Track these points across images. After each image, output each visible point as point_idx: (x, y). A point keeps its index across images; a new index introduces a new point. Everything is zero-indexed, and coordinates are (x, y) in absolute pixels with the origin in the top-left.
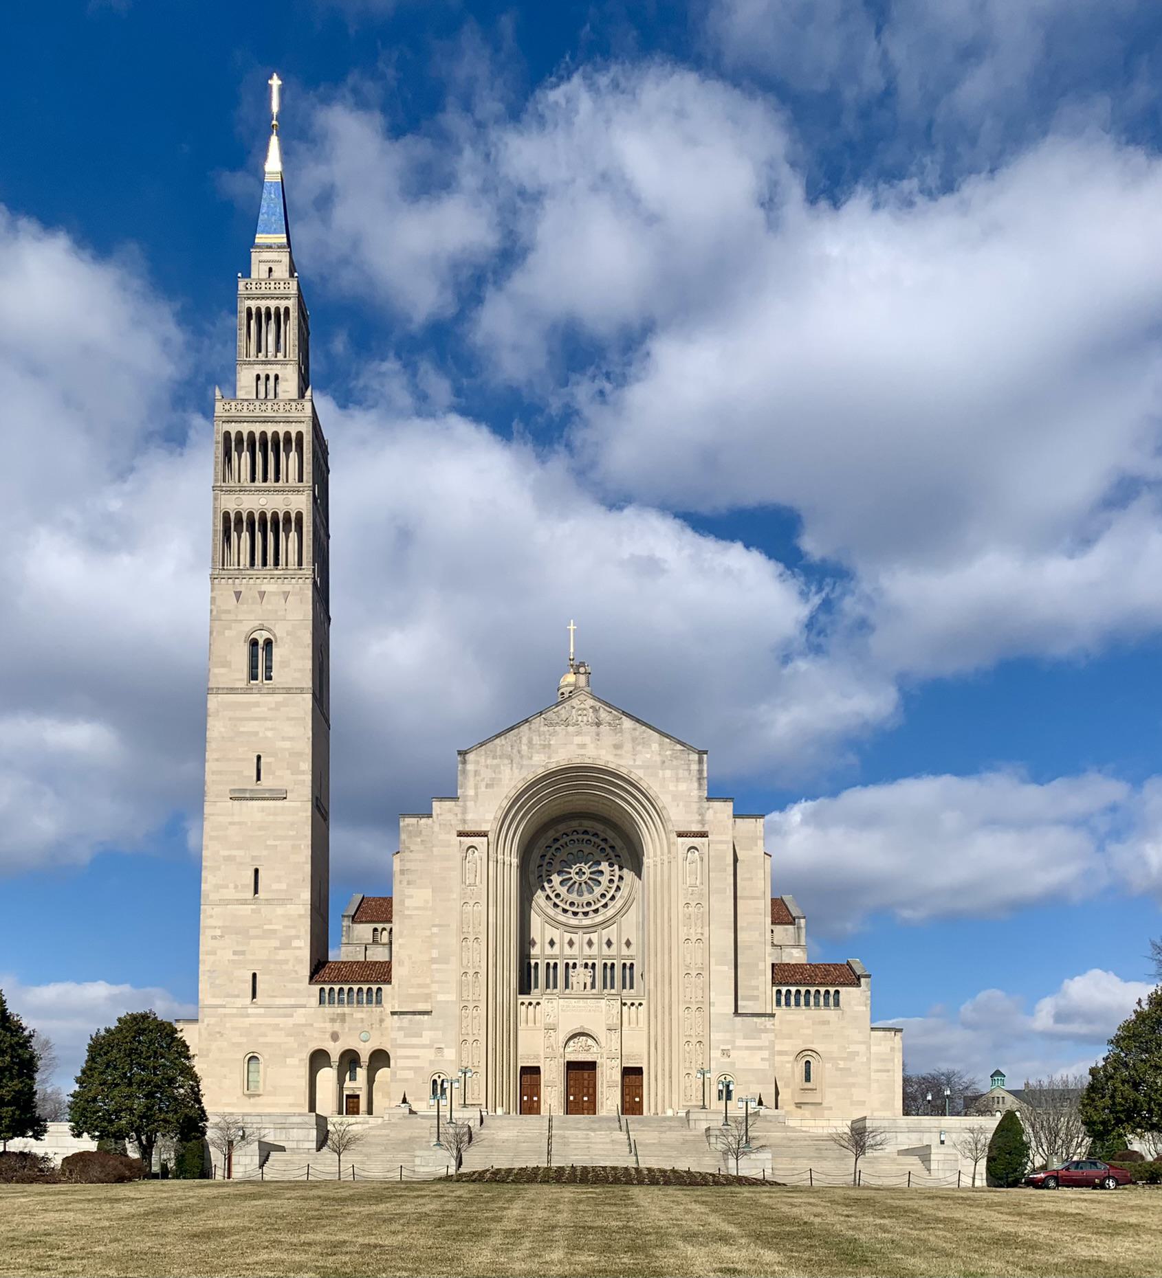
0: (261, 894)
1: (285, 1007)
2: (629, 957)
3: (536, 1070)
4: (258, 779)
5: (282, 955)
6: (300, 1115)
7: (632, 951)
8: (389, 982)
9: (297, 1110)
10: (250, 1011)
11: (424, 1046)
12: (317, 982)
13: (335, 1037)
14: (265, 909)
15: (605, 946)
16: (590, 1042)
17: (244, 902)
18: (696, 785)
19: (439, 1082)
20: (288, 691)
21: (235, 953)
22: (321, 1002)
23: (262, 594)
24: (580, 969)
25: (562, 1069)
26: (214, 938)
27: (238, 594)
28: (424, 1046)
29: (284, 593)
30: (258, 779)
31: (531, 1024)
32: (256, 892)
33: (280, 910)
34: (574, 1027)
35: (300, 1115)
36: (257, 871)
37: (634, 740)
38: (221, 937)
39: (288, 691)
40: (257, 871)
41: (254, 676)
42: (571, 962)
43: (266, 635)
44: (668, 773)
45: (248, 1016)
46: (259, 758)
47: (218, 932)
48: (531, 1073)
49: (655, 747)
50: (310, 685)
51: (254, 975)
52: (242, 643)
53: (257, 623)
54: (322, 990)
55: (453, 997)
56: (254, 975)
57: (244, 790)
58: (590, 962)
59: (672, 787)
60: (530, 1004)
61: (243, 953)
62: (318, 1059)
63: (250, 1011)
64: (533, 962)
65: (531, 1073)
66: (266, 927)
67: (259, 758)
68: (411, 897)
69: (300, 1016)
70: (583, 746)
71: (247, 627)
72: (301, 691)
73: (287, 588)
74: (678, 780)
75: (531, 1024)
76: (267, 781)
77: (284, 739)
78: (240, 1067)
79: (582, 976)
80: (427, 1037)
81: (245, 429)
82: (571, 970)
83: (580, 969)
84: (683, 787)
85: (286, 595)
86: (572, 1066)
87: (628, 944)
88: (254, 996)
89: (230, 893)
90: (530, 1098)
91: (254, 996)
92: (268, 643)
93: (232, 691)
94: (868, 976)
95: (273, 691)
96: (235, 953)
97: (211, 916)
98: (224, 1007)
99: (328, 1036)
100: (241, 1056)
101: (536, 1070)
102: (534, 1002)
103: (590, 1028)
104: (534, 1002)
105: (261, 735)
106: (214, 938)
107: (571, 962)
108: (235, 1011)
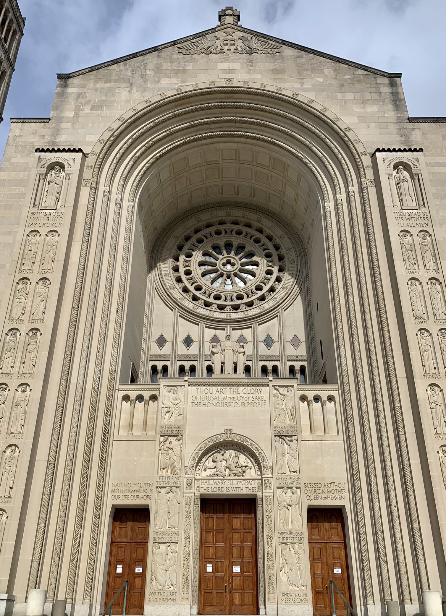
3: (141, 514)
16: (243, 459)
18: (391, 107)
25: (195, 511)
31: (137, 432)
34: (215, 430)
48: (132, 518)
60: (140, 398)
65: (132, 518)
75: (137, 432)
86: (209, 504)
90: (129, 568)
101: (141, 514)
102: (147, 395)
103: (242, 430)
104: (147, 395)
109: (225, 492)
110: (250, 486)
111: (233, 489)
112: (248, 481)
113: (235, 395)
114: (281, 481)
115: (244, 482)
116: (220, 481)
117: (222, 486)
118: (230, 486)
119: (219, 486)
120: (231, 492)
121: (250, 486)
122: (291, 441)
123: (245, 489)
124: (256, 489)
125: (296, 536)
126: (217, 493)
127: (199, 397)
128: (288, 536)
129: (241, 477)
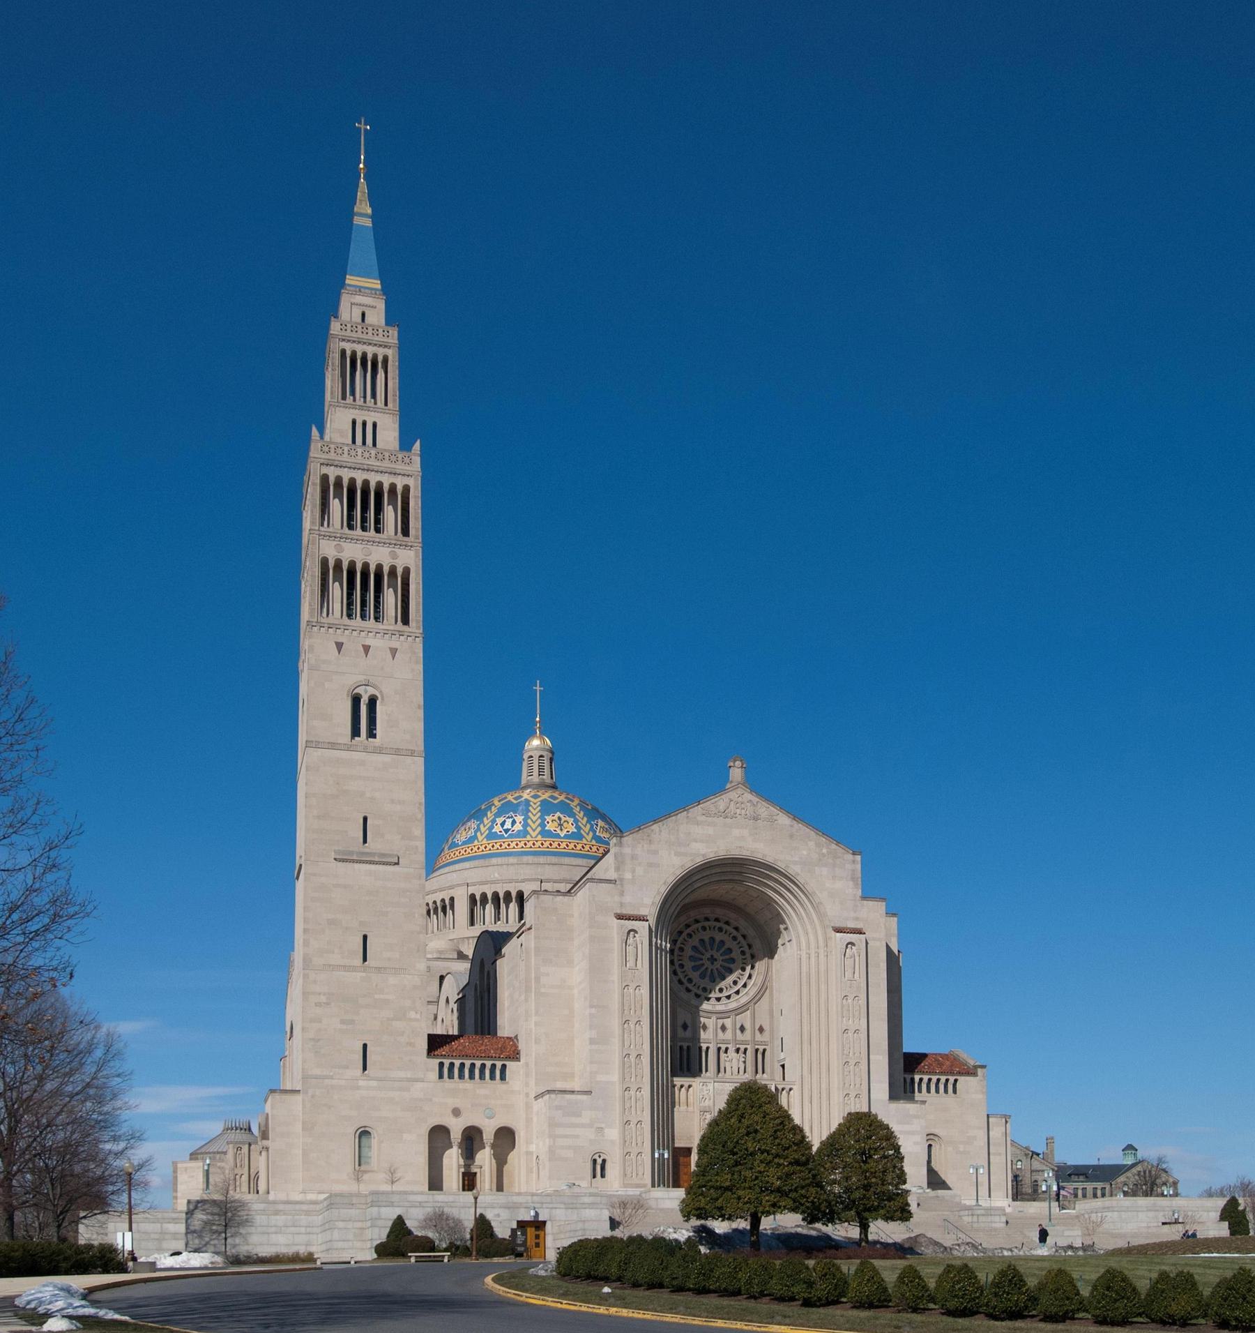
1: (401, 1080)
2: (762, 1043)
4: (365, 841)
5: (398, 1024)
6: (422, 1193)
7: (766, 1037)
8: (518, 1059)
9: (416, 1188)
10: (361, 1083)
11: (583, 1126)
12: (436, 1056)
13: (456, 1112)
15: (738, 1032)
17: (346, 968)
19: (599, 1161)
20: (397, 752)
21: (343, 1022)
22: (441, 1076)
23: (367, 649)
24: (732, 1053)
26: (318, 1004)
27: (339, 646)
28: (583, 1126)
29: (391, 649)
30: (365, 841)
32: (365, 959)
33: (392, 980)
35: (422, 1193)
36: (365, 937)
38: (328, 1004)
39: (397, 752)
40: (365, 937)
41: (356, 732)
42: (723, 1047)
43: (371, 691)
45: (358, 1088)
46: (365, 819)
47: (323, 999)
50: (422, 748)
51: (365, 1046)
52: (345, 696)
53: (361, 678)
54: (441, 1065)
55: (615, 1077)
56: (365, 1046)
57: (351, 853)
58: (742, 1047)
61: (352, 1022)
62: (439, 1135)
63: (361, 1083)
64: (704, 1046)
66: (377, 996)
67: (365, 819)
68: (548, 975)
69: (417, 1090)
71: (350, 680)
73: (394, 644)
76: (374, 844)
77: (392, 801)
78: (350, 1144)
80: (586, 1117)
81: (346, 475)
82: (722, 1055)
83: (732, 1053)
85: (394, 652)
87: (761, 1030)
88: (365, 1068)
91: (365, 1068)
92: (372, 702)
93: (333, 746)
94: (983, 1067)
95: (379, 751)
97: (315, 982)
99: (449, 1111)
100: (350, 1130)
105: (368, 795)
106: (318, 1004)
107: (723, 1047)
108: (343, 1083)
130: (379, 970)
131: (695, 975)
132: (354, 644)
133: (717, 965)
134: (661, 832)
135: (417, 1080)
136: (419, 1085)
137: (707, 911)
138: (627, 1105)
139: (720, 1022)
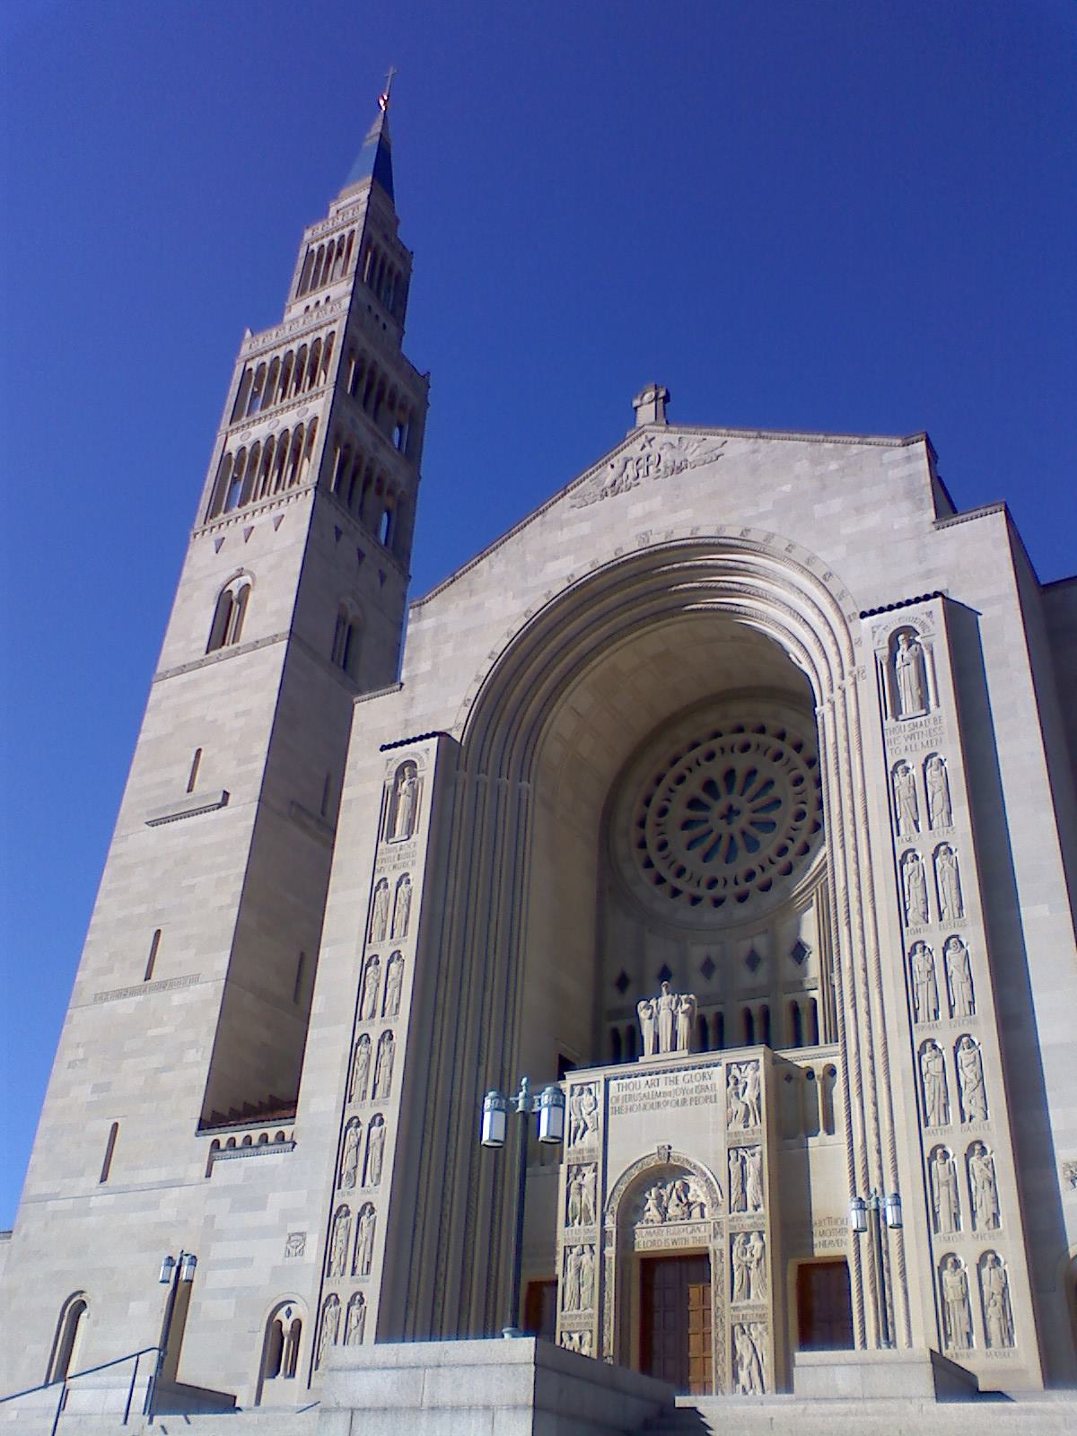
0: (155, 976)
14: (155, 998)
26: (71, 1065)
33: (177, 998)
37: (755, 469)
43: (246, 579)
44: (836, 505)
45: (88, 1212)
49: (802, 467)
59: (848, 529)
61: (105, 1087)
70: (649, 516)
72: (274, 640)
74: (859, 510)
79: (665, 1017)
84: (872, 520)
88: (104, 1178)
89: (114, 981)
91: (104, 1178)
95: (236, 653)
96: (97, 1088)
98: (55, 1196)
106: (71, 1065)
109: (663, 1247)
110: (698, 1234)
111: (674, 1242)
112: (696, 1226)
113: (670, 1088)
114: (735, 1223)
115: (690, 1229)
116: (656, 1229)
117: (659, 1237)
118: (670, 1237)
119: (654, 1237)
120: (671, 1247)
121: (698, 1234)
122: (753, 1155)
123: (691, 1241)
124: (708, 1238)
125: (756, 1312)
126: (651, 1249)
127: (620, 1097)
128: (744, 1312)
129: (686, 1221)
130: (163, 985)
131: (691, 859)
132: (233, 532)
133: (741, 822)
134: (492, 567)
135: (168, 1185)
136: (175, 1192)
137: (712, 719)
138: (347, 1166)
139: (745, 947)
